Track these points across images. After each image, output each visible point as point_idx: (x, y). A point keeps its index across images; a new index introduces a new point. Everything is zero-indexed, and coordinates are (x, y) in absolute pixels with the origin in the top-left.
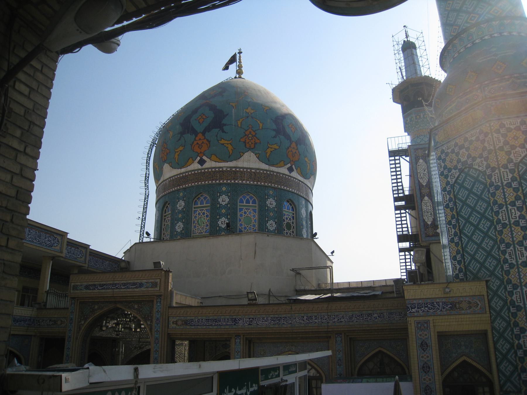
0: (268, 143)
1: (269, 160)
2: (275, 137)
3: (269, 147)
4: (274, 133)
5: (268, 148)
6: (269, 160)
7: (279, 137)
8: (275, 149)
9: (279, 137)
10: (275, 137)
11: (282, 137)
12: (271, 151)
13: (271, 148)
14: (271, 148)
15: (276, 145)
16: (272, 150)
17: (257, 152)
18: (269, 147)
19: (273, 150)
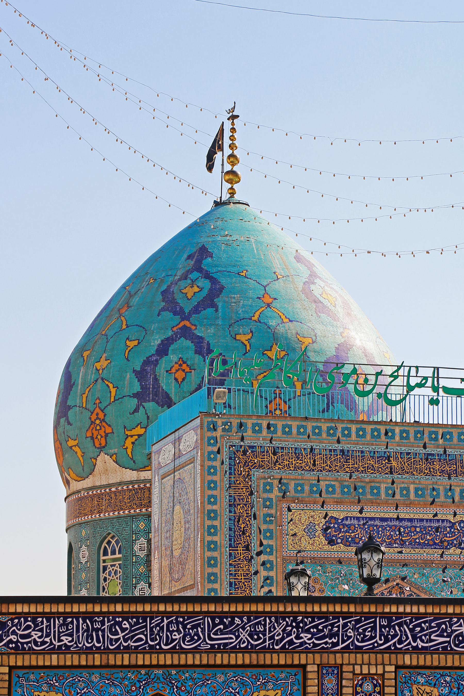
0: (125, 427)
1: (134, 462)
2: (136, 410)
3: (128, 436)
4: (135, 401)
5: (126, 439)
6: (134, 462)
7: (144, 407)
8: (139, 436)
9: (144, 407)
10: (136, 410)
11: (150, 406)
12: (133, 443)
13: (132, 436)
14: (132, 436)
15: (139, 427)
16: (133, 439)
17: (112, 451)
18: (128, 436)
19: (136, 440)
